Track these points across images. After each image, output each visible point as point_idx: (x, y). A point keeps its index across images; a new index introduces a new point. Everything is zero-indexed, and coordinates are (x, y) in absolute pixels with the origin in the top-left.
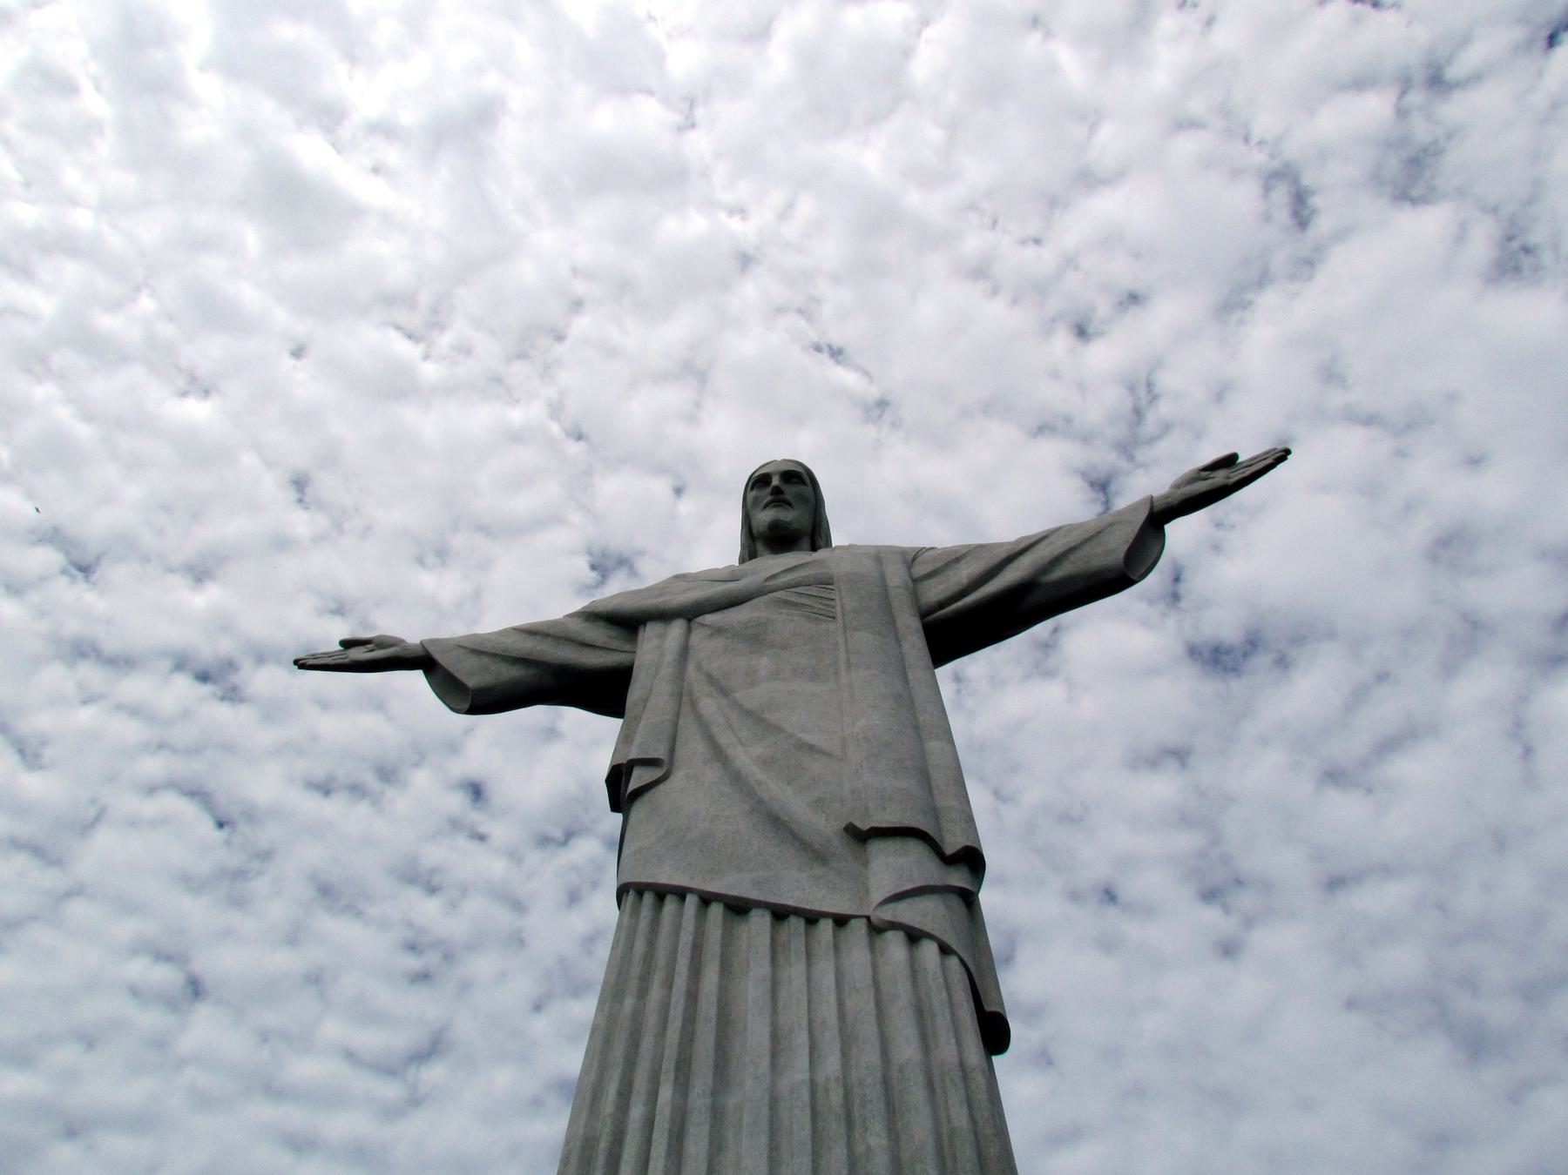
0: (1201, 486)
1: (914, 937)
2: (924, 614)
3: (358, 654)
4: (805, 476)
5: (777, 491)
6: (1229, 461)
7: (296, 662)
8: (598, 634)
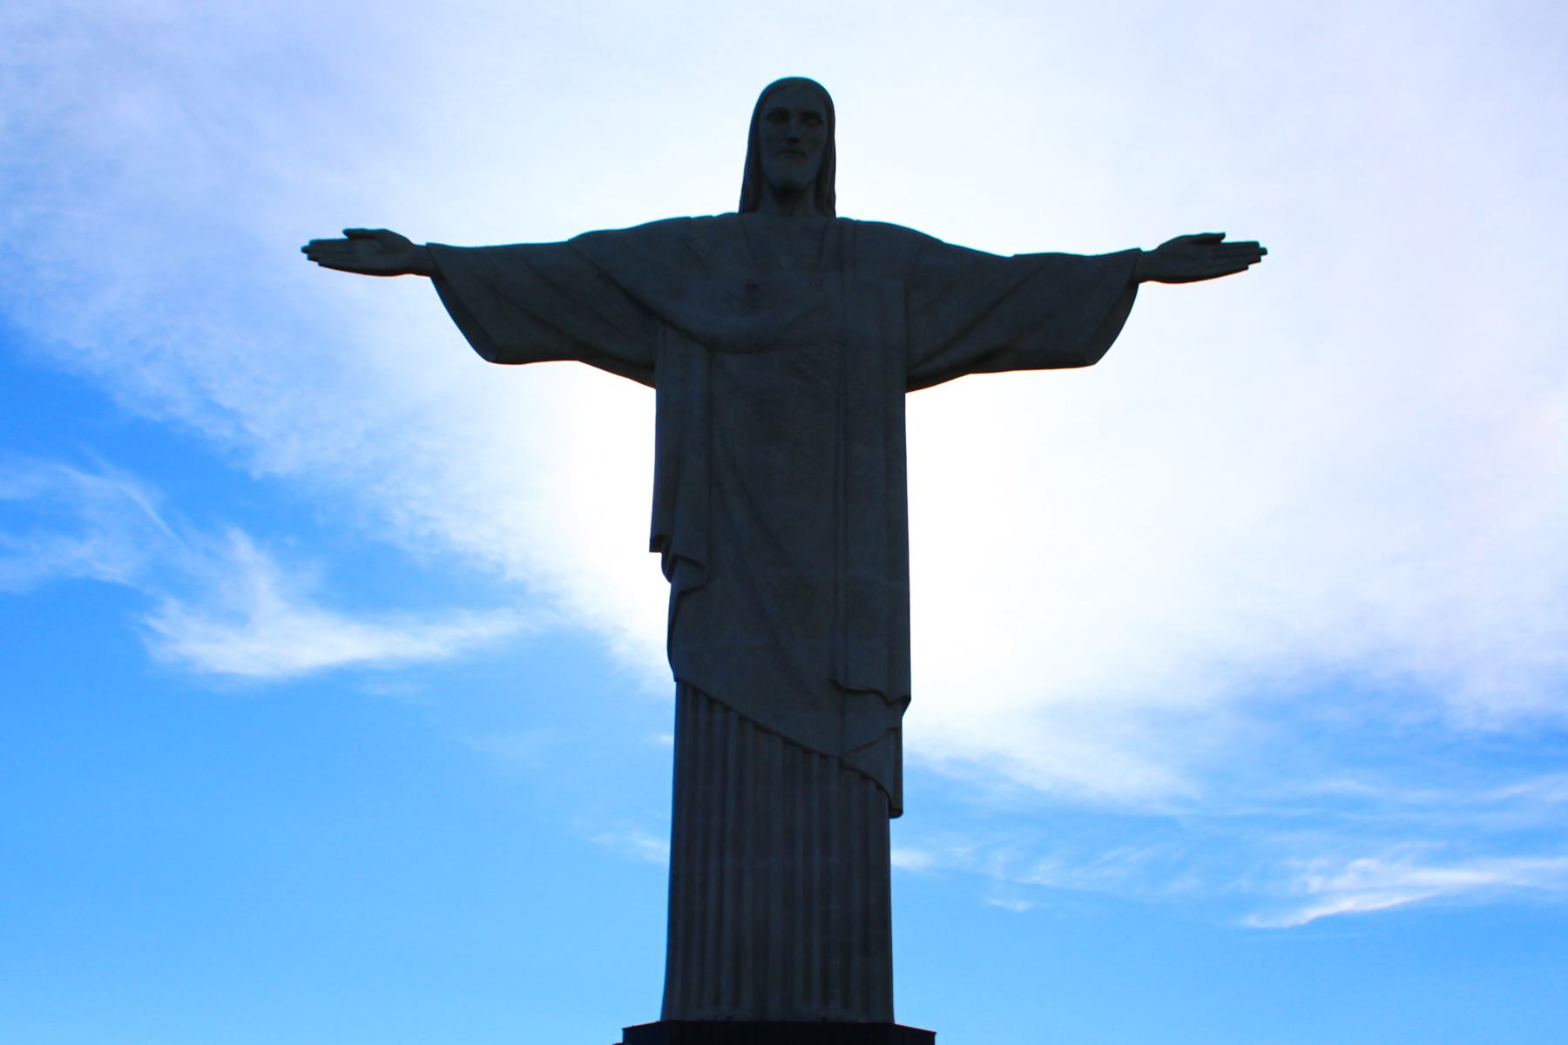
1: (864, 777)
4: (824, 118)
5: (794, 141)
6: (1212, 241)
7: (305, 250)
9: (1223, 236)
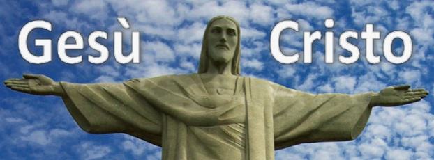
0: (393, 99)
2: (275, 137)
3: (33, 85)
4: (236, 32)
5: (223, 41)
8: (144, 110)
9: (409, 87)
